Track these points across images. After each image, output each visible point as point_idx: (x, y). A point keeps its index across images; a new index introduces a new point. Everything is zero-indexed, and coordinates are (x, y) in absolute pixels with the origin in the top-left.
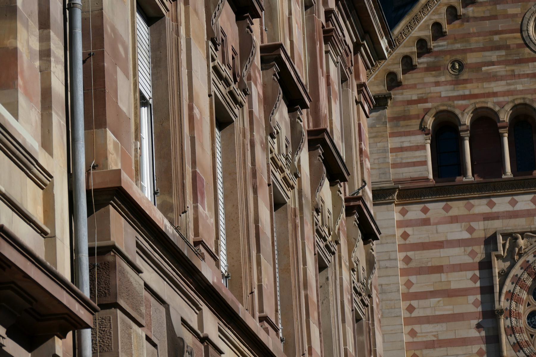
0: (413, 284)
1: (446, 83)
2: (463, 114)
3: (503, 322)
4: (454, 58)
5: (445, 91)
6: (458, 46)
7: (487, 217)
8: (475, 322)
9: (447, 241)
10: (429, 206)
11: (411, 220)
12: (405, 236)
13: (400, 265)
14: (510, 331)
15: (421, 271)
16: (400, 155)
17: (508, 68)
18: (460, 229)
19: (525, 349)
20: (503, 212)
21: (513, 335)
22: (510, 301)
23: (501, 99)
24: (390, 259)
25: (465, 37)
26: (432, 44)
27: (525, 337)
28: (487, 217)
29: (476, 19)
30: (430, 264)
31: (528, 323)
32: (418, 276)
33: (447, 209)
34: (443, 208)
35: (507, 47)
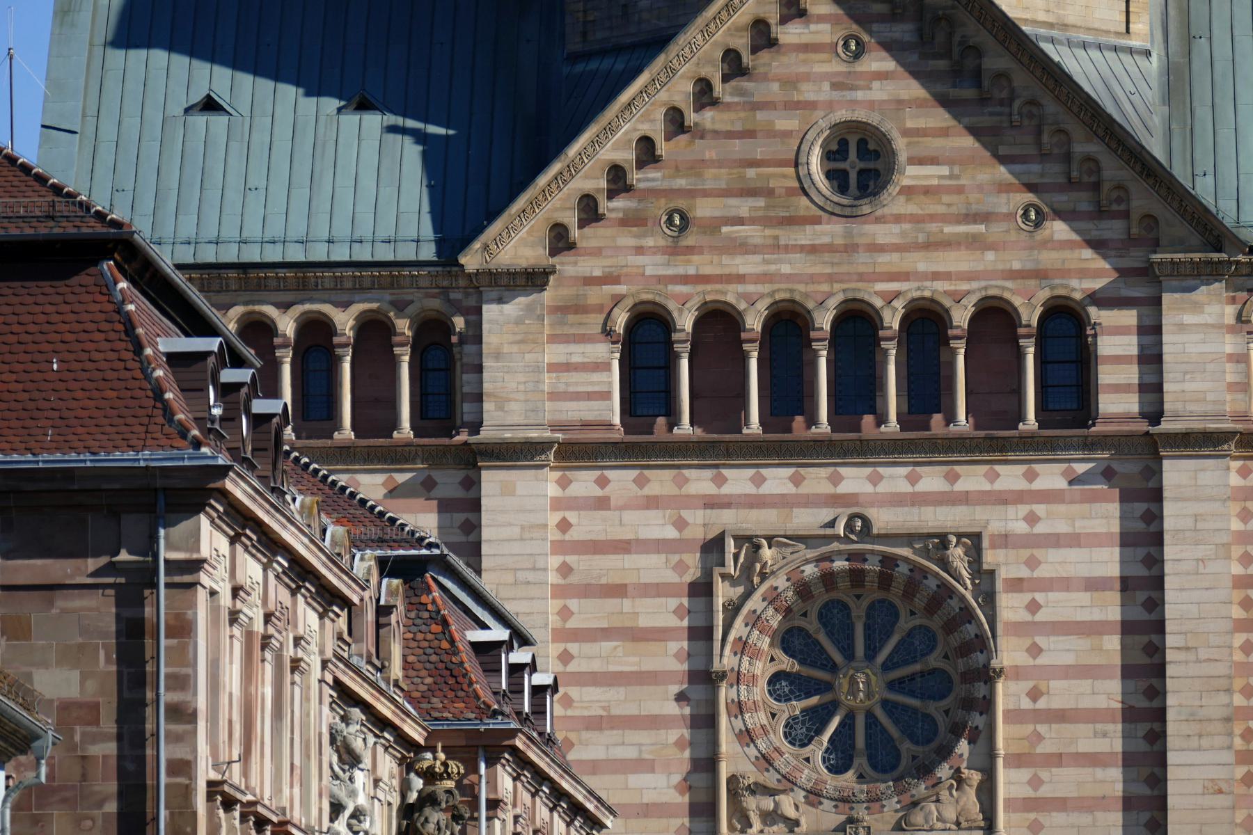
0: (573, 613)
1: (656, 250)
2: (681, 311)
3: (725, 693)
4: (672, 205)
5: (653, 265)
6: (681, 183)
7: (711, 503)
8: (675, 689)
9: (637, 540)
10: (610, 474)
11: (576, 498)
12: (564, 526)
13: (553, 578)
14: (735, 710)
15: (588, 591)
16: (567, 377)
17: (768, 232)
18: (661, 522)
19: (759, 742)
20: (740, 496)
21: (740, 717)
22: (739, 655)
23: (751, 288)
24: (534, 569)
25: (696, 167)
26: (635, 177)
27: (762, 718)
28: (711, 503)
29: (716, 134)
30: (604, 581)
31: (769, 691)
32: (582, 601)
33: (641, 482)
34: (634, 481)
35: (769, 193)
